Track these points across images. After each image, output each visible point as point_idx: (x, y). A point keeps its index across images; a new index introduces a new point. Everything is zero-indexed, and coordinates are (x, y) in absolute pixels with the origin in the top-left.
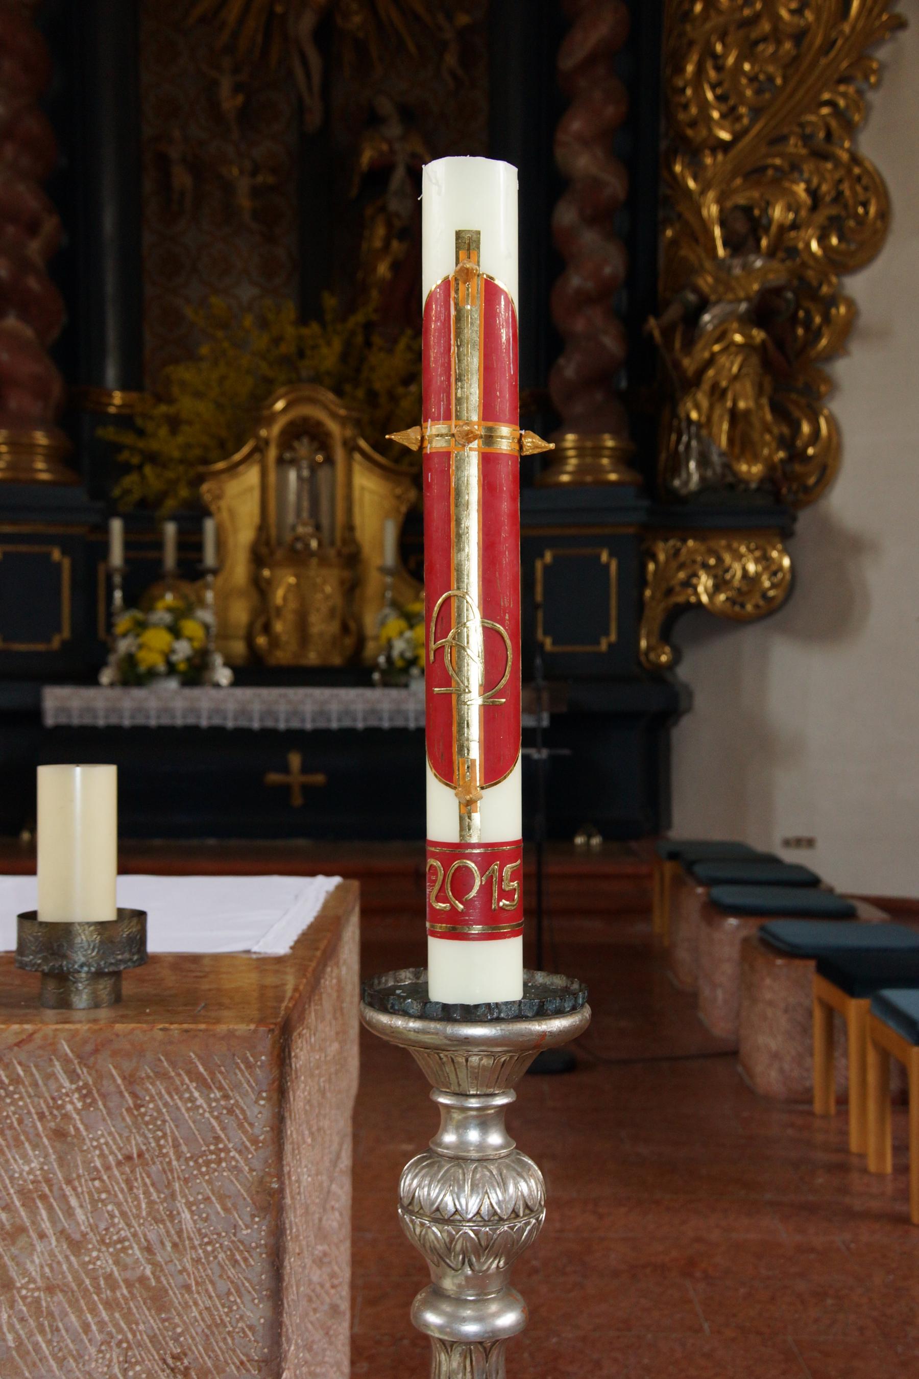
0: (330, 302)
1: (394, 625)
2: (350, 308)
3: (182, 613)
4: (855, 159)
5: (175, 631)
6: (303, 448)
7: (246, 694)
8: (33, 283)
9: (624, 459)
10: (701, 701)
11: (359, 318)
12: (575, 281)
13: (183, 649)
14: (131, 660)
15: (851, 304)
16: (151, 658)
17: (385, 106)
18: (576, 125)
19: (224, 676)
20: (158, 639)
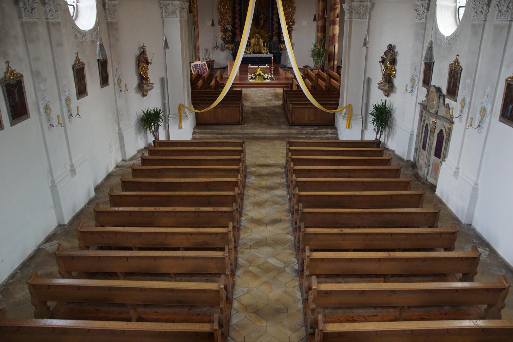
0: (258, 27)
1: (263, 51)
2: (259, 27)
3: (250, 49)
4: (293, 18)
5: (249, 51)
6: (256, 38)
7: (254, 55)
8: (239, 27)
9: (278, 39)
10: (283, 54)
11: (260, 28)
12: (275, 27)
13: (250, 52)
14: (247, 53)
15: (293, 28)
16: (248, 53)
17: (261, 13)
18: (275, 16)
19: (252, 53)
20: (249, 51)
